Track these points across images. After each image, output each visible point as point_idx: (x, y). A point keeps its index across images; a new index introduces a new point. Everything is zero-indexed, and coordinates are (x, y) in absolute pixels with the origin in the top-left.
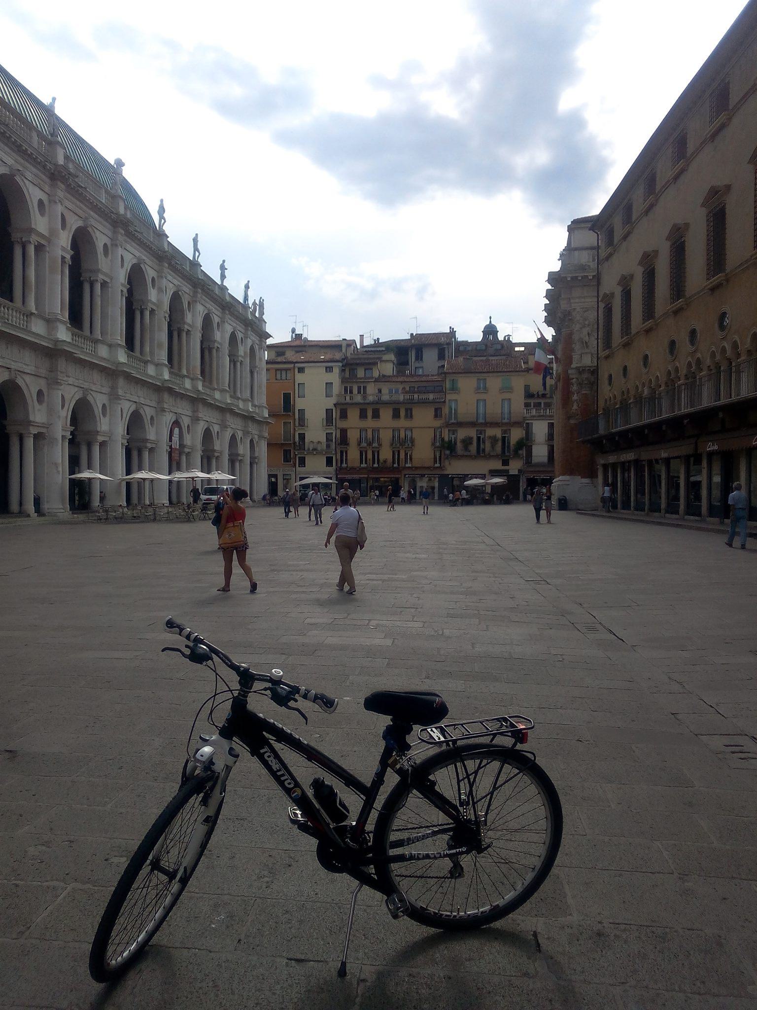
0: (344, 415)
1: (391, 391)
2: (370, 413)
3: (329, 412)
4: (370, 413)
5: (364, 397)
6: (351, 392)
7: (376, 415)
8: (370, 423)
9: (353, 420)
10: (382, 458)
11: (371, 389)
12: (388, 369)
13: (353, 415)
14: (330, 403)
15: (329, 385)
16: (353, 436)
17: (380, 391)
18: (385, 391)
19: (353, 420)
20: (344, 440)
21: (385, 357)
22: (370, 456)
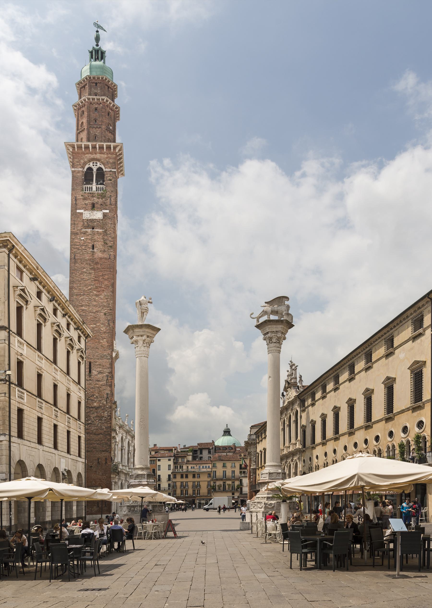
0: (175, 477)
1: (192, 467)
2: (184, 476)
3: (169, 476)
4: (184, 476)
5: (182, 470)
6: (177, 468)
7: (187, 477)
8: (184, 480)
9: (178, 479)
10: (189, 493)
11: (185, 467)
12: (190, 458)
13: (178, 477)
14: (170, 472)
15: (169, 466)
16: (178, 484)
17: (188, 467)
18: (190, 467)
19: (178, 479)
20: (175, 486)
21: (188, 454)
22: (184, 492)
